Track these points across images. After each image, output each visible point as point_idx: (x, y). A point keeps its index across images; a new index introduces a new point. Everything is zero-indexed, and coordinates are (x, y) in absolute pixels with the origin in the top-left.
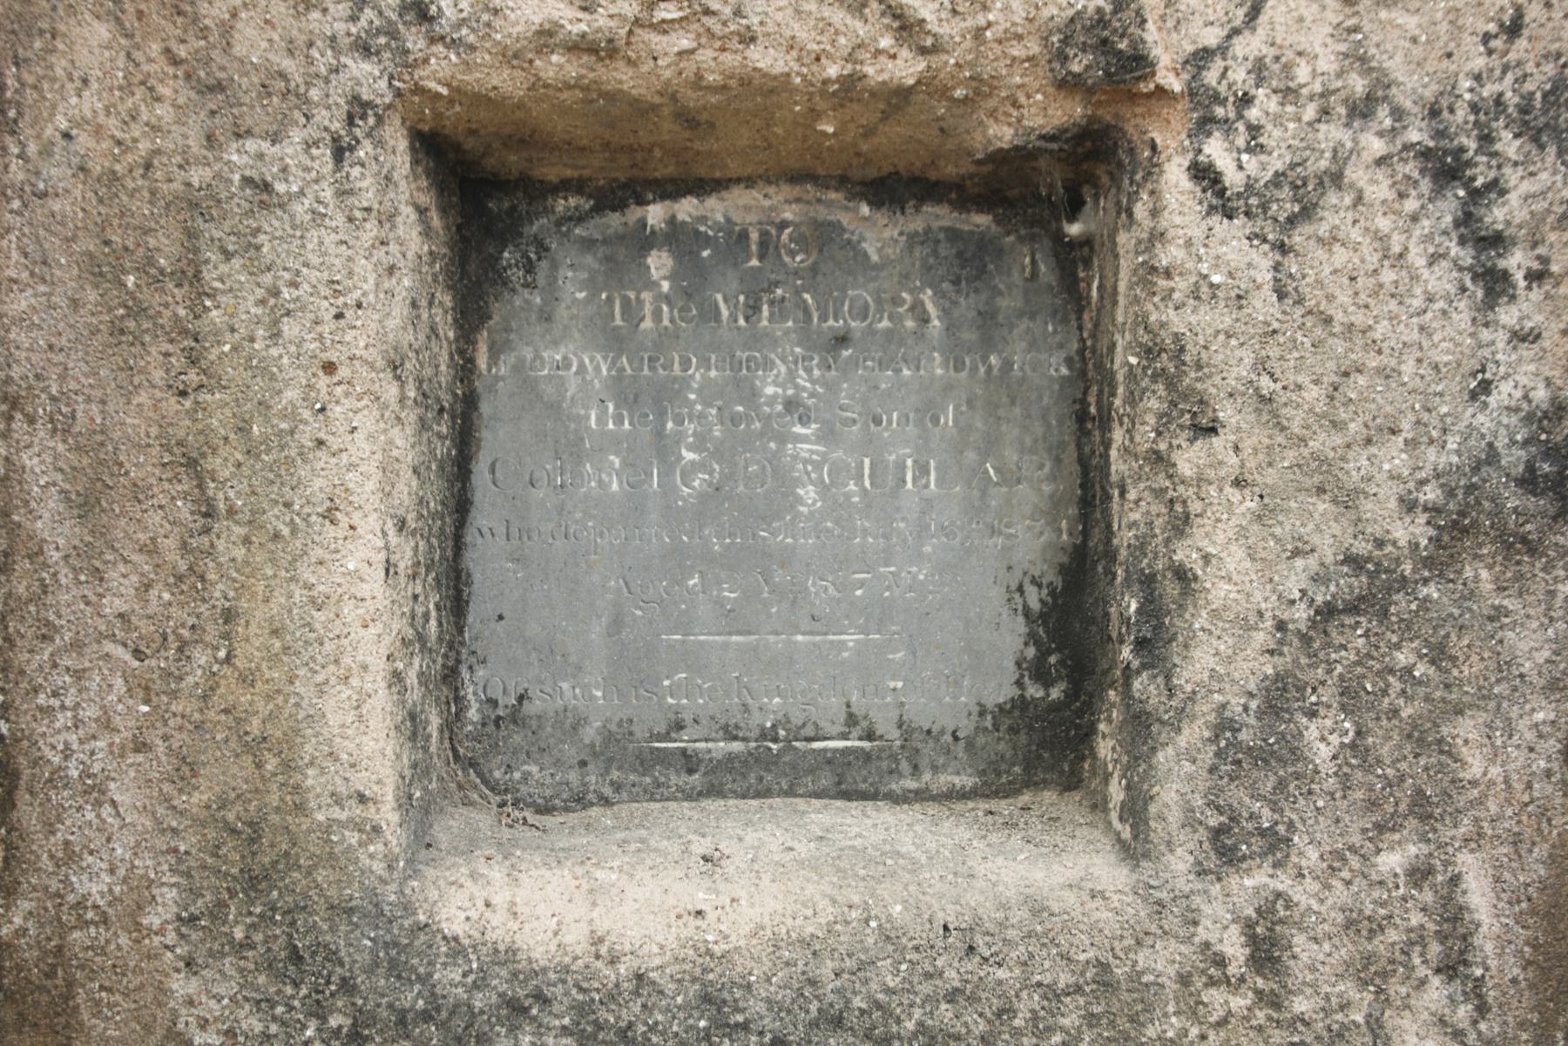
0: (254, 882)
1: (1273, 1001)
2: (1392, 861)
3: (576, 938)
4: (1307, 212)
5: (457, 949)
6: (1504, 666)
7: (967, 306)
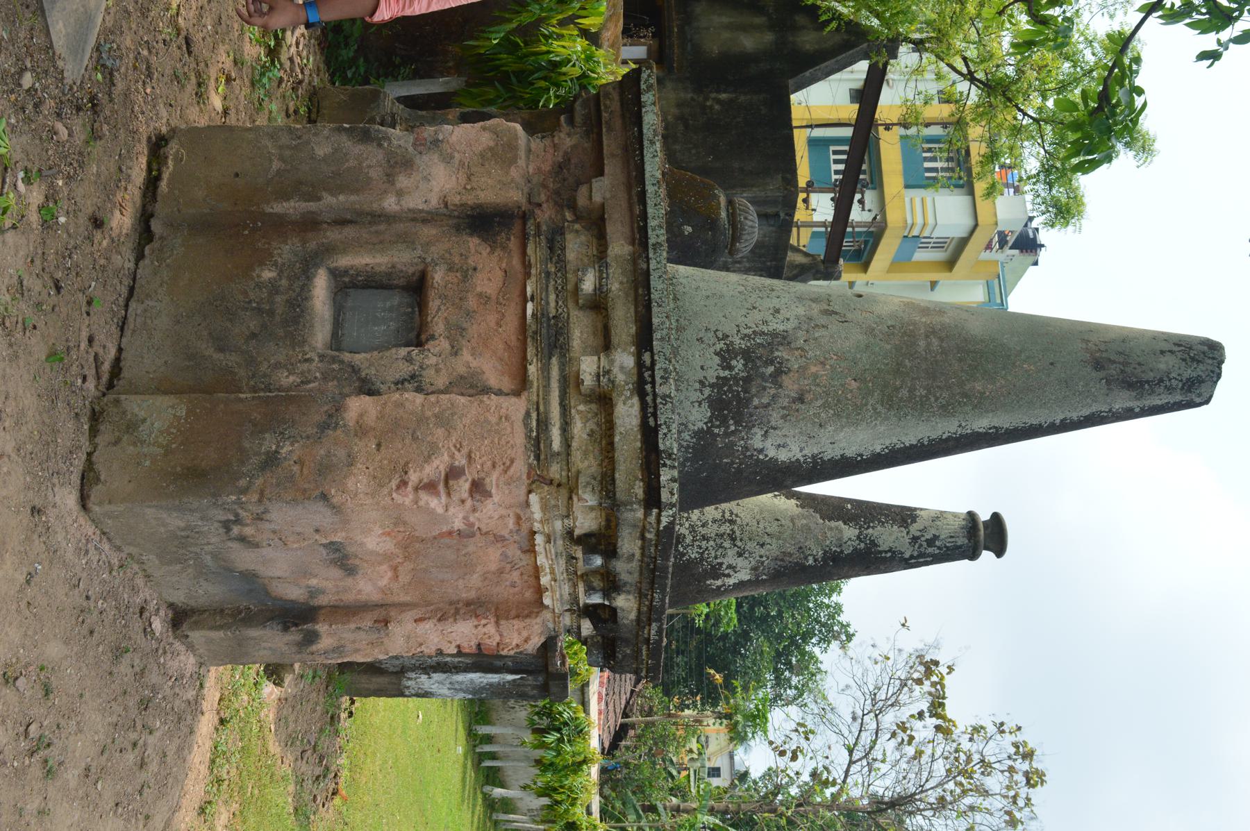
1: (300, 361)
2: (318, 374)
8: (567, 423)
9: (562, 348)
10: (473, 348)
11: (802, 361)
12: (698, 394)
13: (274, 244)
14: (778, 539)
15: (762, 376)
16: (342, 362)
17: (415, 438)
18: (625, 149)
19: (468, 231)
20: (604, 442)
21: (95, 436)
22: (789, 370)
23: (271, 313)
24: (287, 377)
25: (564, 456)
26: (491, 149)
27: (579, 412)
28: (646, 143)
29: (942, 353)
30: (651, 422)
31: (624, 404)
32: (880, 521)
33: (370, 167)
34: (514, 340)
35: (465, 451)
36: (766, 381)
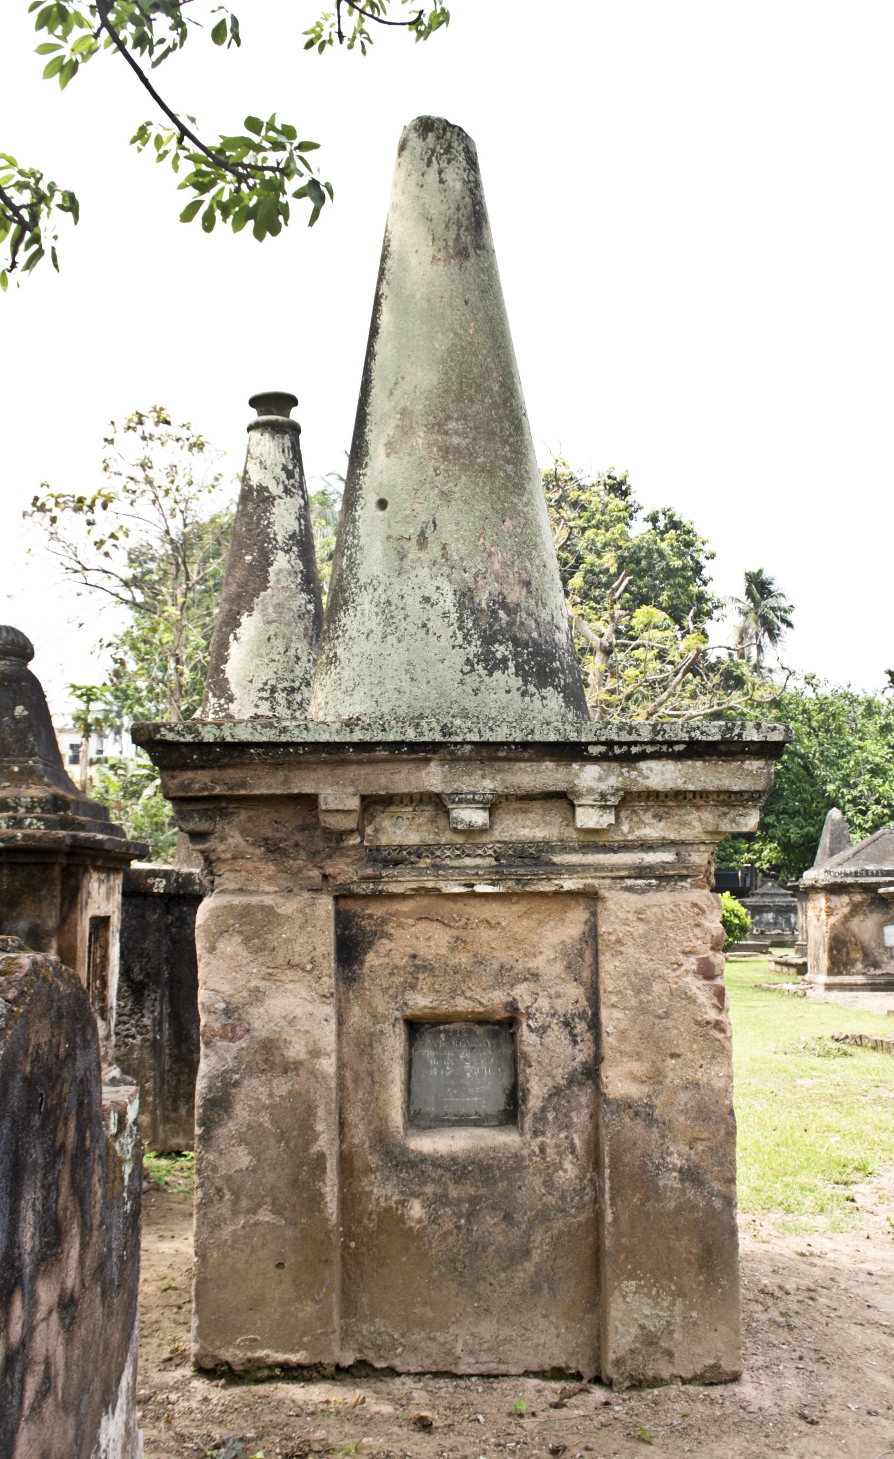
0: (381, 1141)
1: (543, 1159)
2: (562, 1135)
3: (431, 1150)
4: (545, 1032)
5: (413, 1151)
6: (579, 1104)
7: (494, 1042)
8: (642, 845)
9: (542, 851)
10: (526, 956)
11: (491, 578)
12: (535, 698)
13: (371, 1207)
14: (290, 640)
15: (511, 624)
16: (544, 1109)
17: (667, 1015)
18: (277, 765)
19: (356, 967)
20: (671, 803)
21: (662, 1380)
22: (501, 593)
23: (474, 1200)
24: (565, 1171)
25: (682, 849)
26: (247, 940)
27: (631, 831)
28: (283, 738)
29: (466, 420)
30: (681, 747)
31: (647, 778)
32: (268, 526)
33: (271, 1095)
34: (519, 908)
35: (682, 958)
36: (515, 621)
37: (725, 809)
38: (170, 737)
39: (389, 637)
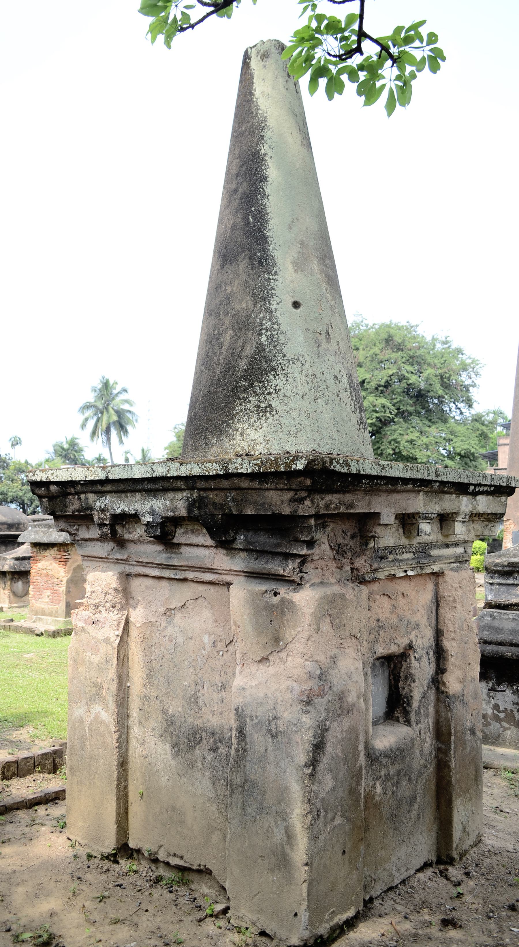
16: (419, 707)
37: (487, 523)
38: (338, 468)
39: (319, 400)
